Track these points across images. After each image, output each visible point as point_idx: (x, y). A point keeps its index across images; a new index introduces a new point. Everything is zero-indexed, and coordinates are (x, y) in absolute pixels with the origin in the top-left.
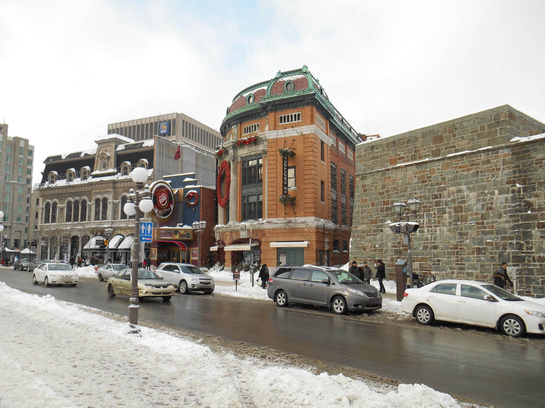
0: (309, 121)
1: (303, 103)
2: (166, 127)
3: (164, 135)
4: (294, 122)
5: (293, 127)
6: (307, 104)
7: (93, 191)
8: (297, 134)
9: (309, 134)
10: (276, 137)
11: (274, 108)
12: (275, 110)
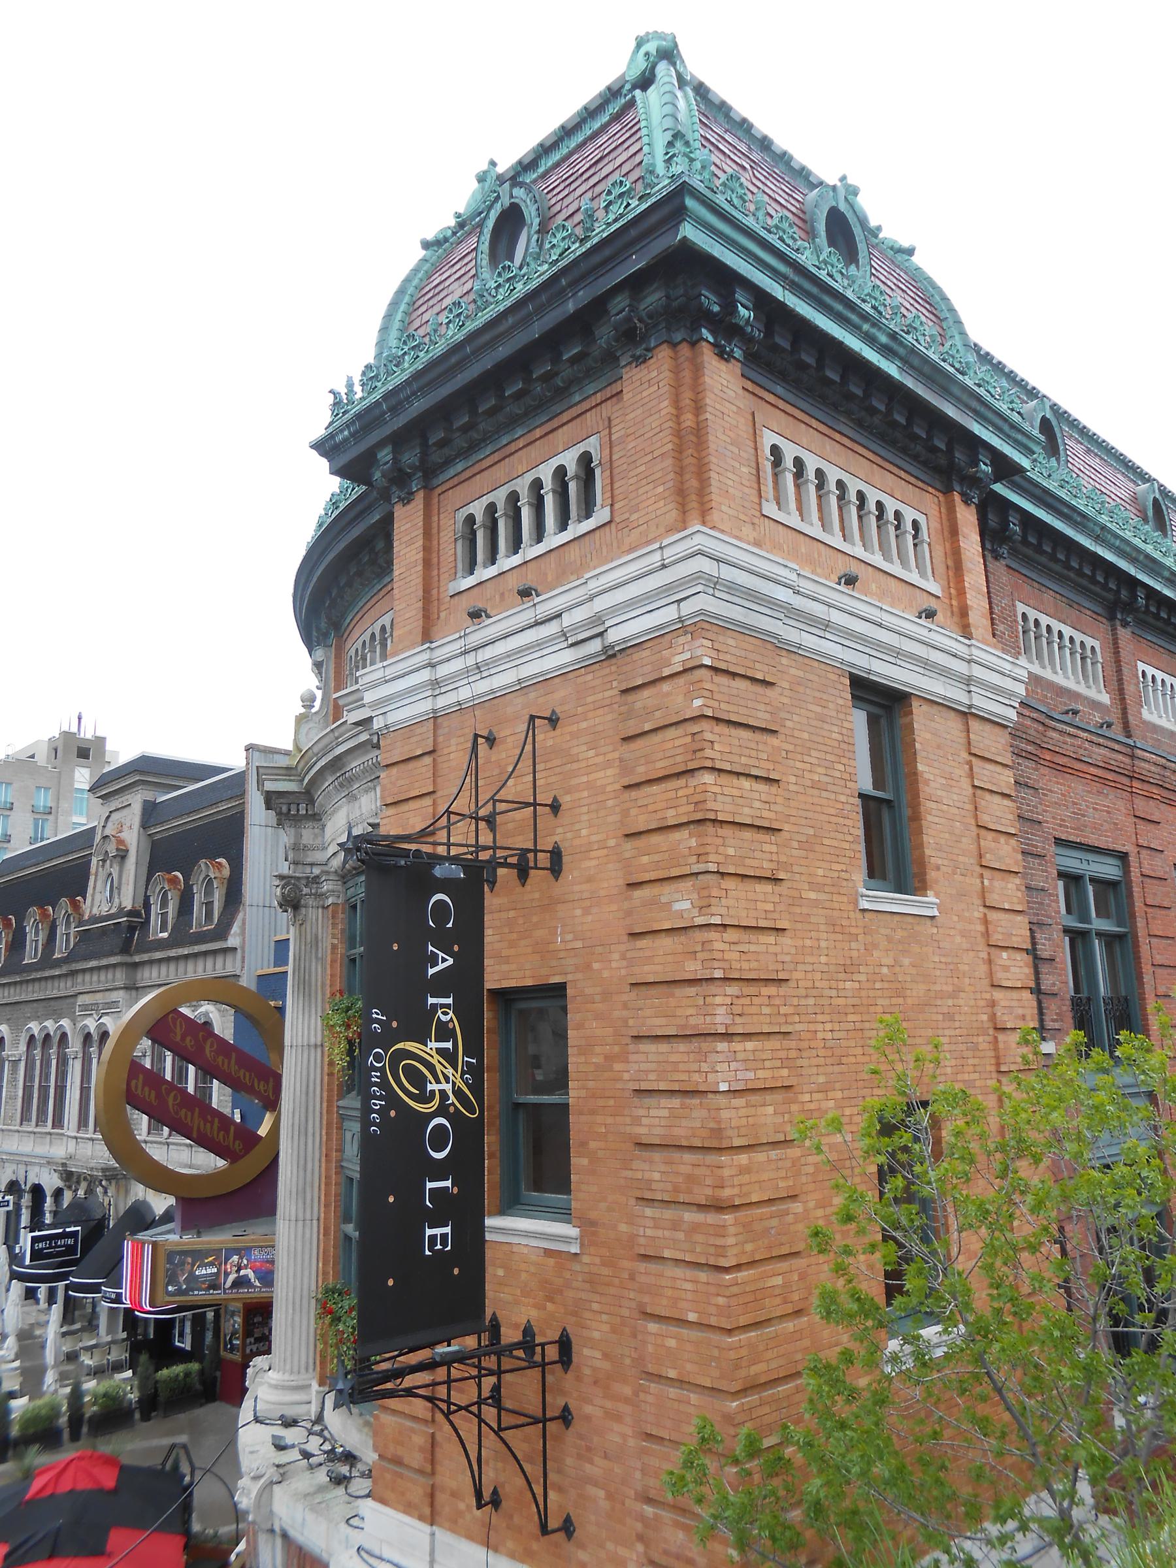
0: (656, 501)
1: (604, 335)
4: (554, 539)
5: (525, 593)
6: (634, 341)
7: (81, 1000)
8: (567, 657)
9: (660, 637)
10: (425, 706)
11: (410, 457)
12: (430, 473)
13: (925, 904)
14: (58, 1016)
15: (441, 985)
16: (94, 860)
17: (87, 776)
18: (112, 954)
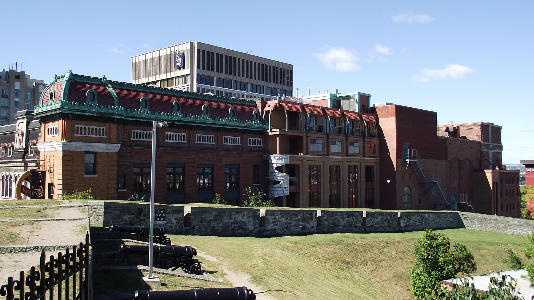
2: (180, 59)
3: (180, 68)
13: (96, 175)
14: (9, 171)
15: (40, 183)
16: (16, 135)
17: (19, 85)
18: (20, 158)
